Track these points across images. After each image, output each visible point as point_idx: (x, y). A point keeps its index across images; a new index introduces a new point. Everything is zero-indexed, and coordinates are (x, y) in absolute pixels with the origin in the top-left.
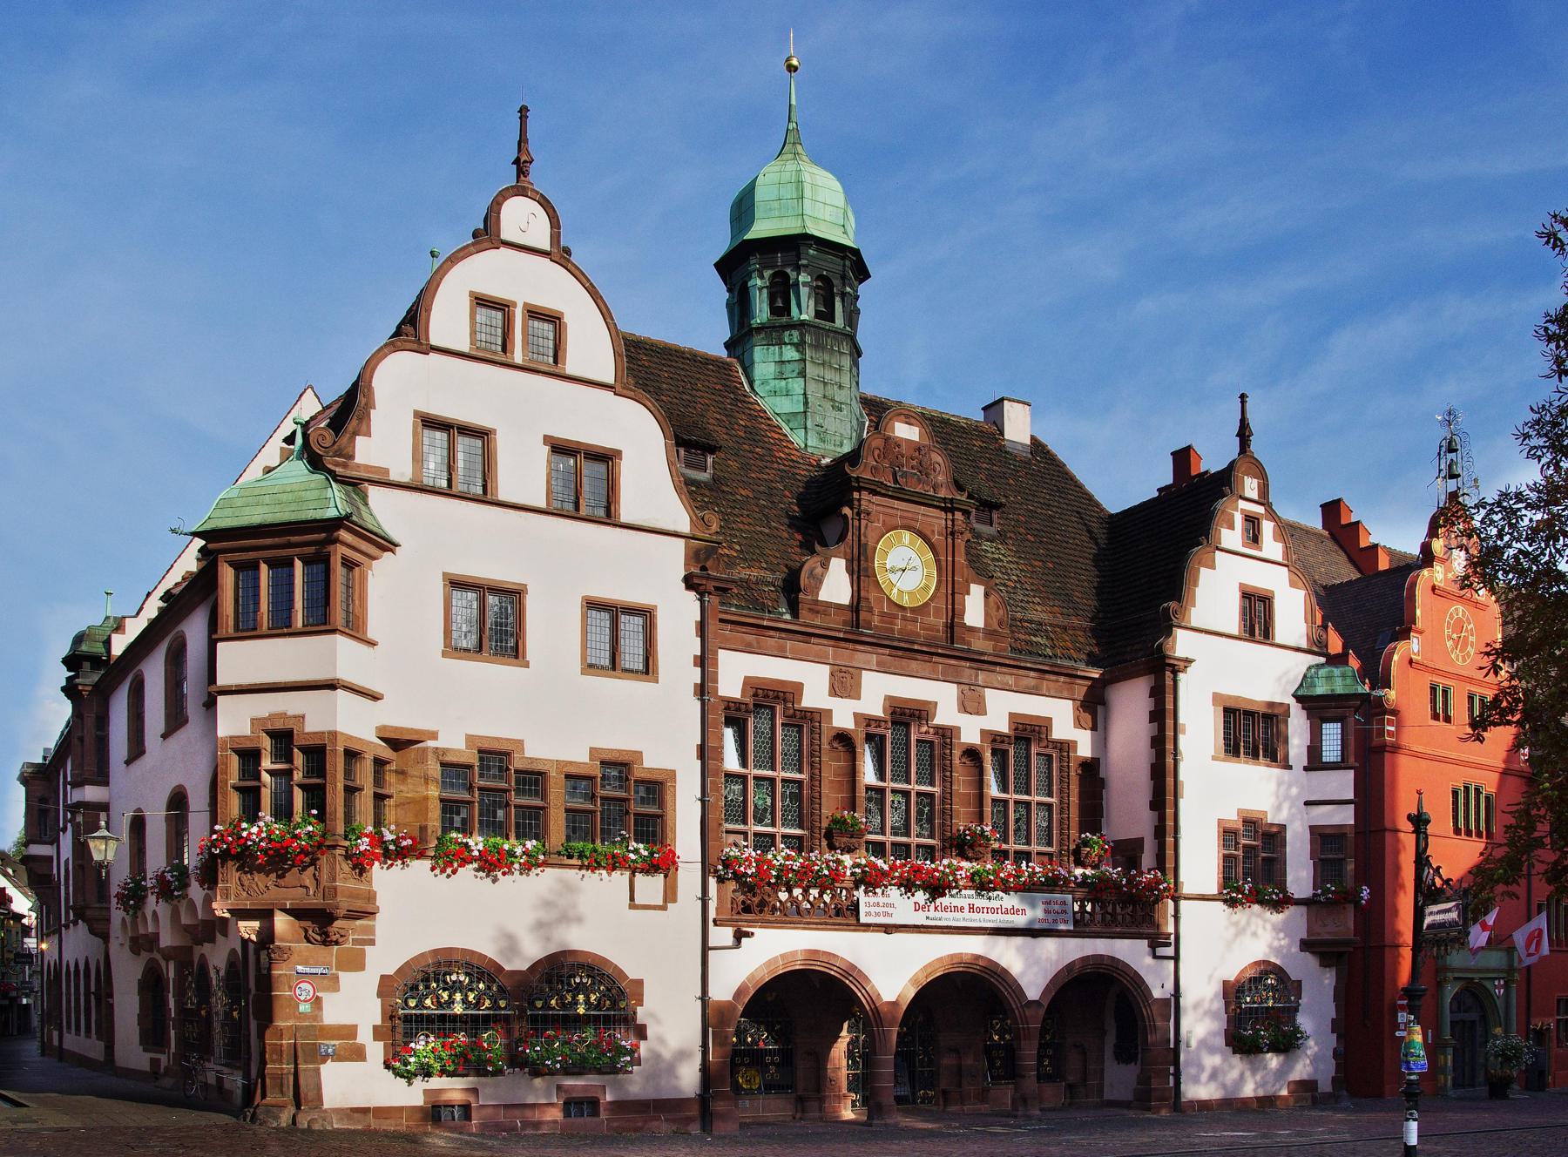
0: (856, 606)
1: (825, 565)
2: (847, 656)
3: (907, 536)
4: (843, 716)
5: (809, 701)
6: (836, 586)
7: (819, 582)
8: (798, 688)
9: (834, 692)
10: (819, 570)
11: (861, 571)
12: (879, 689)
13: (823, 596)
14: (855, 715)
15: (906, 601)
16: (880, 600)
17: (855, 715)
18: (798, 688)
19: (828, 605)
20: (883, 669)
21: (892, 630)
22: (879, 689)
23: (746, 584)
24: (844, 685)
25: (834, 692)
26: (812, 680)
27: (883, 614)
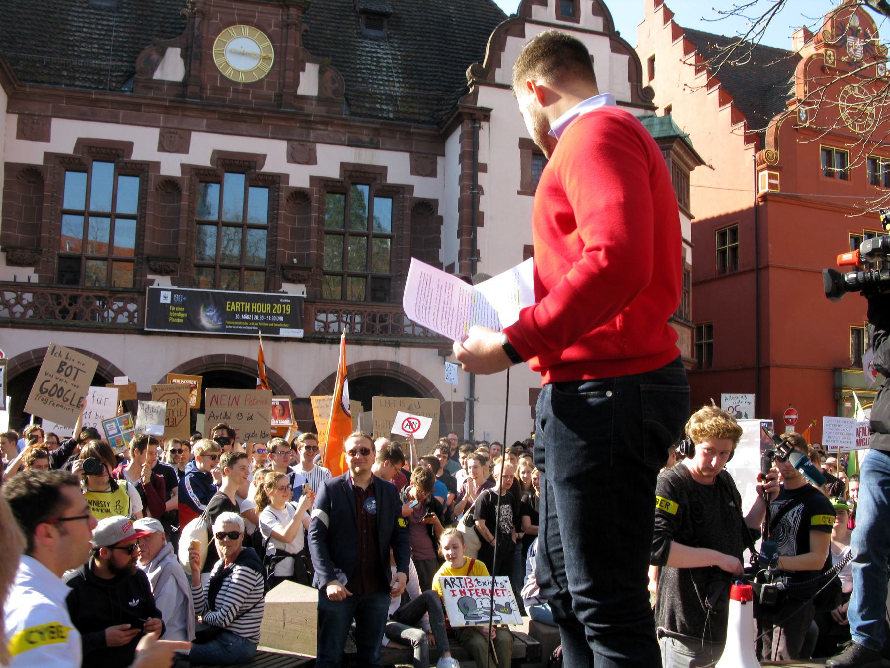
0: (184, 84)
1: (162, 54)
2: (174, 122)
3: (246, 29)
4: (171, 165)
5: (137, 155)
6: (172, 67)
7: (154, 66)
8: (129, 146)
9: (162, 148)
10: (155, 57)
11: (197, 55)
12: (203, 147)
13: (157, 75)
14: (183, 166)
15: (242, 79)
16: (215, 78)
17: (183, 166)
18: (129, 146)
19: (161, 82)
20: (212, 129)
21: (225, 100)
22: (203, 147)
23: (98, 71)
24: (174, 142)
25: (162, 148)
26: (144, 142)
27: (215, 89)
